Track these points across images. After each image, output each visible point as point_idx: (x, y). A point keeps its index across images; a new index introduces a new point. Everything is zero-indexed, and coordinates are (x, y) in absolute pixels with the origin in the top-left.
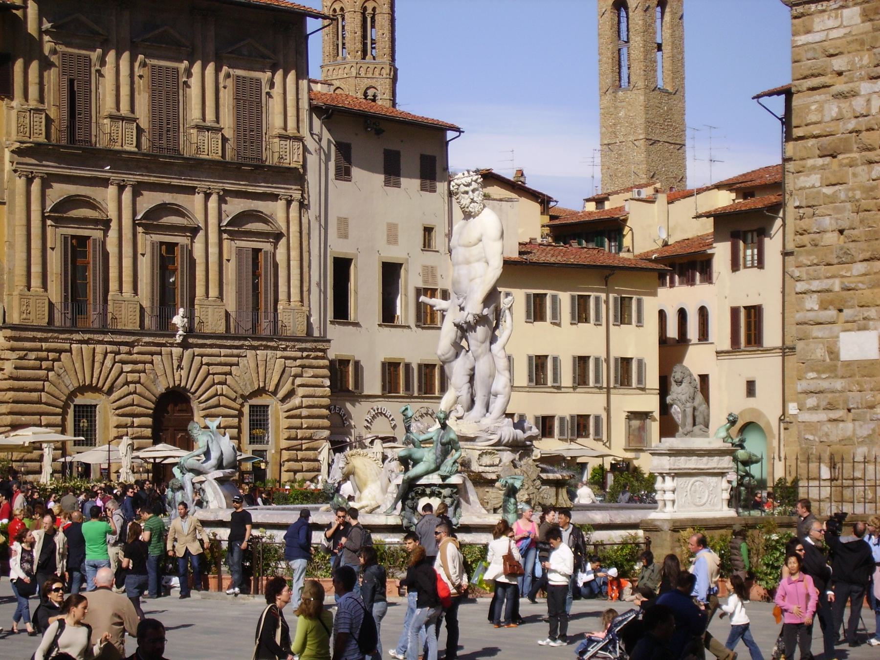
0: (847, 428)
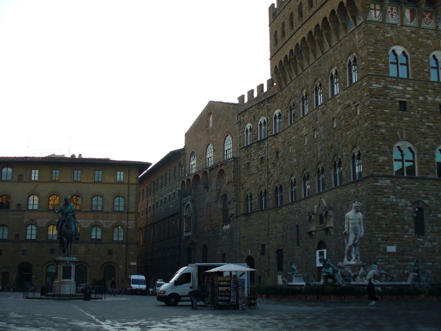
0: (389, 266)
